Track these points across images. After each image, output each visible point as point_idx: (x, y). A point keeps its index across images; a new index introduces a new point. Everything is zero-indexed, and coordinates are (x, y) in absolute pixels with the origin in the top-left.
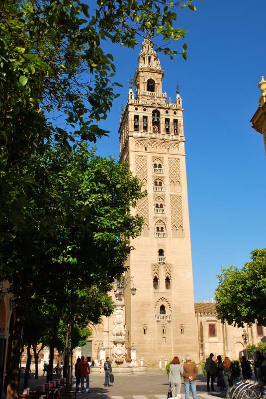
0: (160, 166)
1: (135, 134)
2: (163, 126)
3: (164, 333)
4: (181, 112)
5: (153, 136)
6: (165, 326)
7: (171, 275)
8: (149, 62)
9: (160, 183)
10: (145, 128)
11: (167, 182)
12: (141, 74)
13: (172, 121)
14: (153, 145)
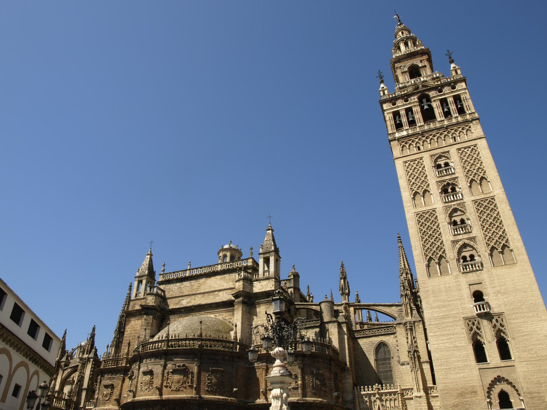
0: (447, 164)
2: (438, 112)
4: (463, 84)
5: (426, 128)
11: (462, 184)
13: (450, 100)
14: (428, 140)
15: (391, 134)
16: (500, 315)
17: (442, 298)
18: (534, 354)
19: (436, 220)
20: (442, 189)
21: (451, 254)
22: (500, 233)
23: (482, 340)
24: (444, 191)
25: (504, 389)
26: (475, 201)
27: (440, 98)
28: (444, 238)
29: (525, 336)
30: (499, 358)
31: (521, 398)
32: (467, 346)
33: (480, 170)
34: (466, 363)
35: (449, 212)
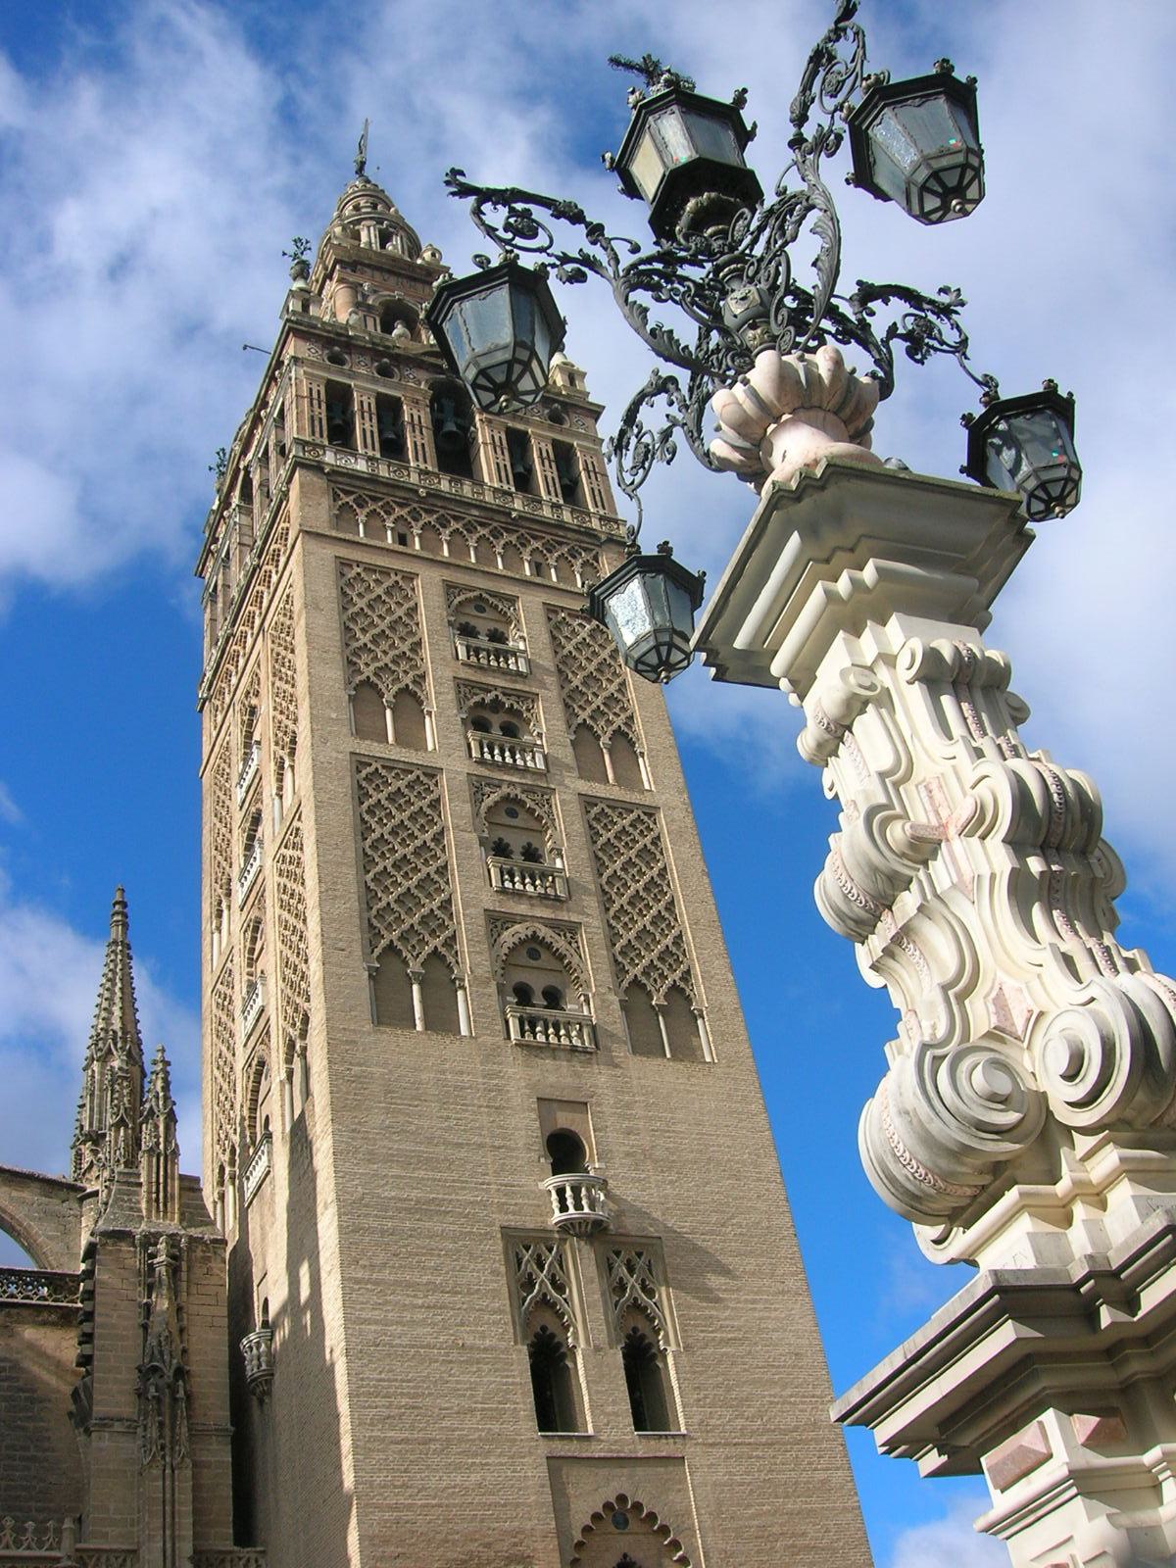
1: (329, 458)
5: (444, 485)
10: (393, 448)
17: (426, 1123)
18: (751, 1419)
26: (588, 802)
27: (510, 424)
28: (457, 888)
29: (727, 1342)
30: (631, 1420)
32: (506, 1351)
34: (496, 1427)
35: (489, 801)
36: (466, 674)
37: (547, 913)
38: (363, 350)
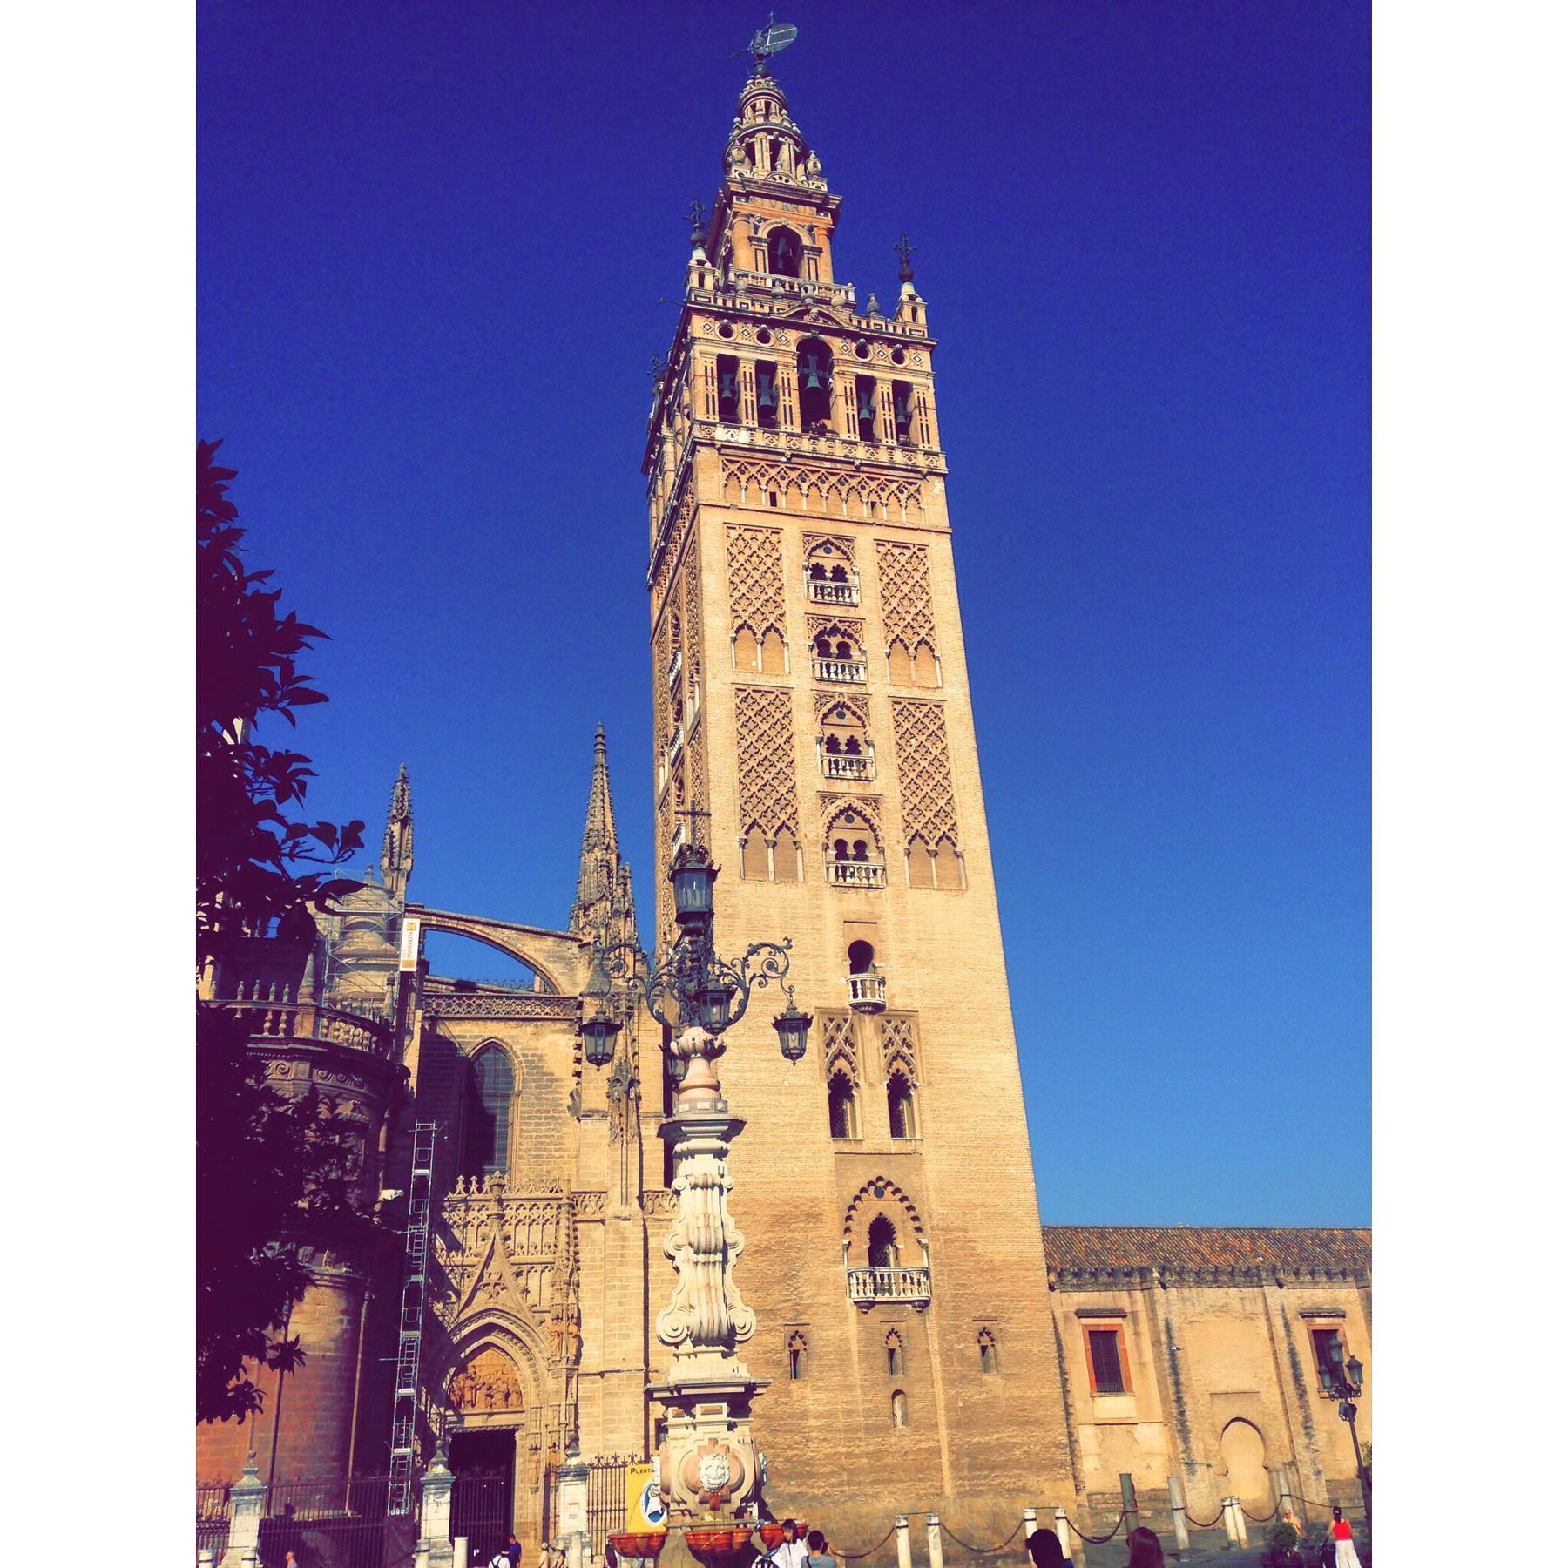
0: (839, 574)
1: (721, 434)
2: (843, 411)
3: (892, 1371)
4: (925, 356)
5: (806, 445)
6: (900, 1327)
7: (916, 1062)
8: (774, 159)
9: (841, 646)
10: (767, 417)
11: (873, 641)
12: (739, 205)
13: (884, 389)
15: (703, 423)
16: (906, 1017)
19: (785, 722)
20: (816, 638)
21: (811, 827)
22: (941, 803)
23: (851, 1075)
24: (821, 646)
25: (888, 1214)
27: (860, 372)
31: (924, 1241)
33: (920, 618)
34: (805, 1135)
35: (825, 710)
36: (814, 609)
37: (860, 791)
38: (746, 319)
